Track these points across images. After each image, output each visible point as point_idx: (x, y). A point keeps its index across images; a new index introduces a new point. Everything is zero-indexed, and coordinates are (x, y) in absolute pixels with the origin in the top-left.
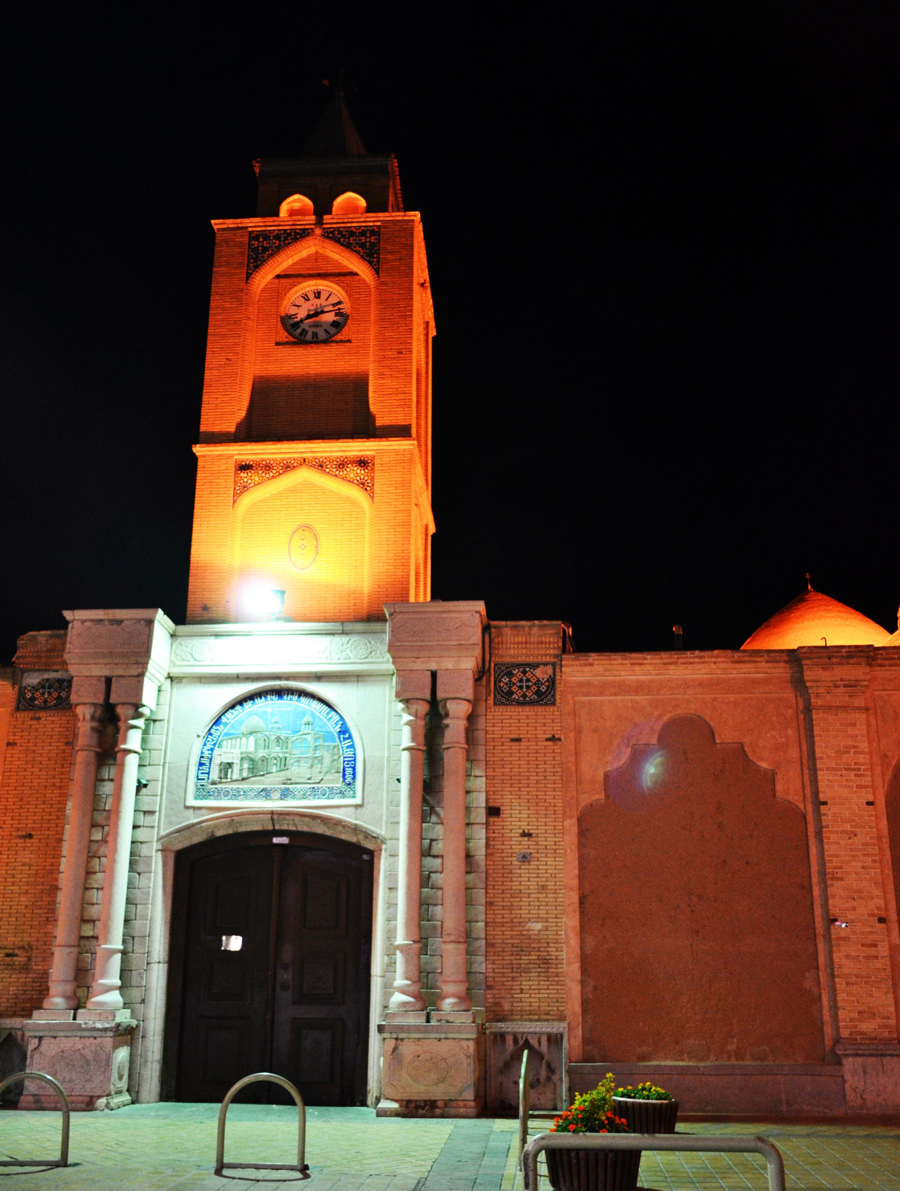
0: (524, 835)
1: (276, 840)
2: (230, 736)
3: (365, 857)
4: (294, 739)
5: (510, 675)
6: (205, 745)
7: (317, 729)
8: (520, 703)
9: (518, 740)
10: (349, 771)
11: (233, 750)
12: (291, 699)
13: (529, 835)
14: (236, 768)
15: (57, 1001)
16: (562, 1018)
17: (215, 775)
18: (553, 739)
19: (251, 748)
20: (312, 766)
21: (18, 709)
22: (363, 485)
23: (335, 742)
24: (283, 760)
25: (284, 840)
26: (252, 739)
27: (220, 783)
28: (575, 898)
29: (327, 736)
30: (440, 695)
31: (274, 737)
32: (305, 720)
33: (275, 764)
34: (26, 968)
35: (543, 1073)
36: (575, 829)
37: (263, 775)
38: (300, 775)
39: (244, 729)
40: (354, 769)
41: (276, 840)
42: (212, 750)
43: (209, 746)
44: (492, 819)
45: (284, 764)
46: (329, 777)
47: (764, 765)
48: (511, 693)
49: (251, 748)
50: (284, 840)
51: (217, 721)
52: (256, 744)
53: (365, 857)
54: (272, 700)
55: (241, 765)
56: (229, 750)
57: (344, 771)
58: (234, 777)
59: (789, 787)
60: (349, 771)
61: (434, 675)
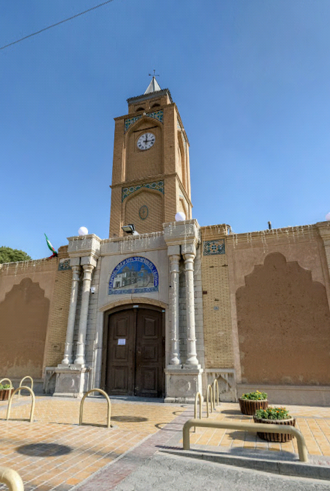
0: (216, 300)
1: (135, 306)
2: (118, 273)
3: (163, 311)
5: (209, 245)
8: (212, 254)
9: (213, 267)
13: (218, 300)
15: (67, 361)
16: (233, 367)
17: (114, 286)
18: (225, 266)
21: (59, 270)
22: (161, 190)
25: (137, 306)
30: (182, 253)
34: (60, 351)
35: (227, 389)
36: (234, 297)
41: (135, 306)
44: (205, 295)
47: (306, 269)
48: (209, 251)
50: (137, 306)
51: (115, 269)
53: (163, 311)
59: (317, 276)
60: (156, 281)
61: (180, 246)
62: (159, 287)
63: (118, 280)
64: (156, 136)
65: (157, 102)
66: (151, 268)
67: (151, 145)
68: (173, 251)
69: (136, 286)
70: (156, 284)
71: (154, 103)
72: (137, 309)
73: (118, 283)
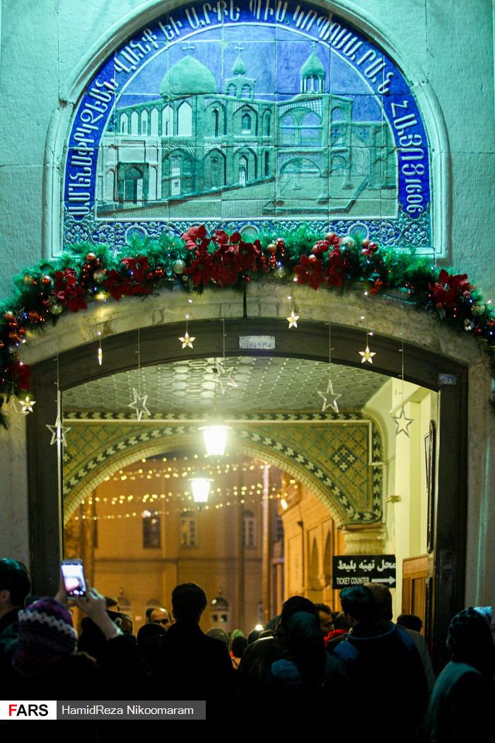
4: (283, 110)
6: (78, 123)
7: (335, 88)
10: (414, 184)
11: (144, 137)
12: (271, 19)
20: (328, 173)
23: (379, 119)
24: (262, 159)
26: (186, 111)
27: (120, 210)
29: (358, 104)
31: (236, 106)
32: (305, 67)
33: (242, 168)
37: (218, 193)
38: (302, 192)
39: (164, 86)
40: (425, 180)
42: (96, 135)
43: (88, 127)
45: (264, 167)
46: (367, 196)
49: (186, 132)
52: (195, 120)
54: (227, 19)
55: (166, 171)
56: (134, 135)
57: (402, 184)
58: (151, 197)
60: (414, 184)
63: (129, 156)
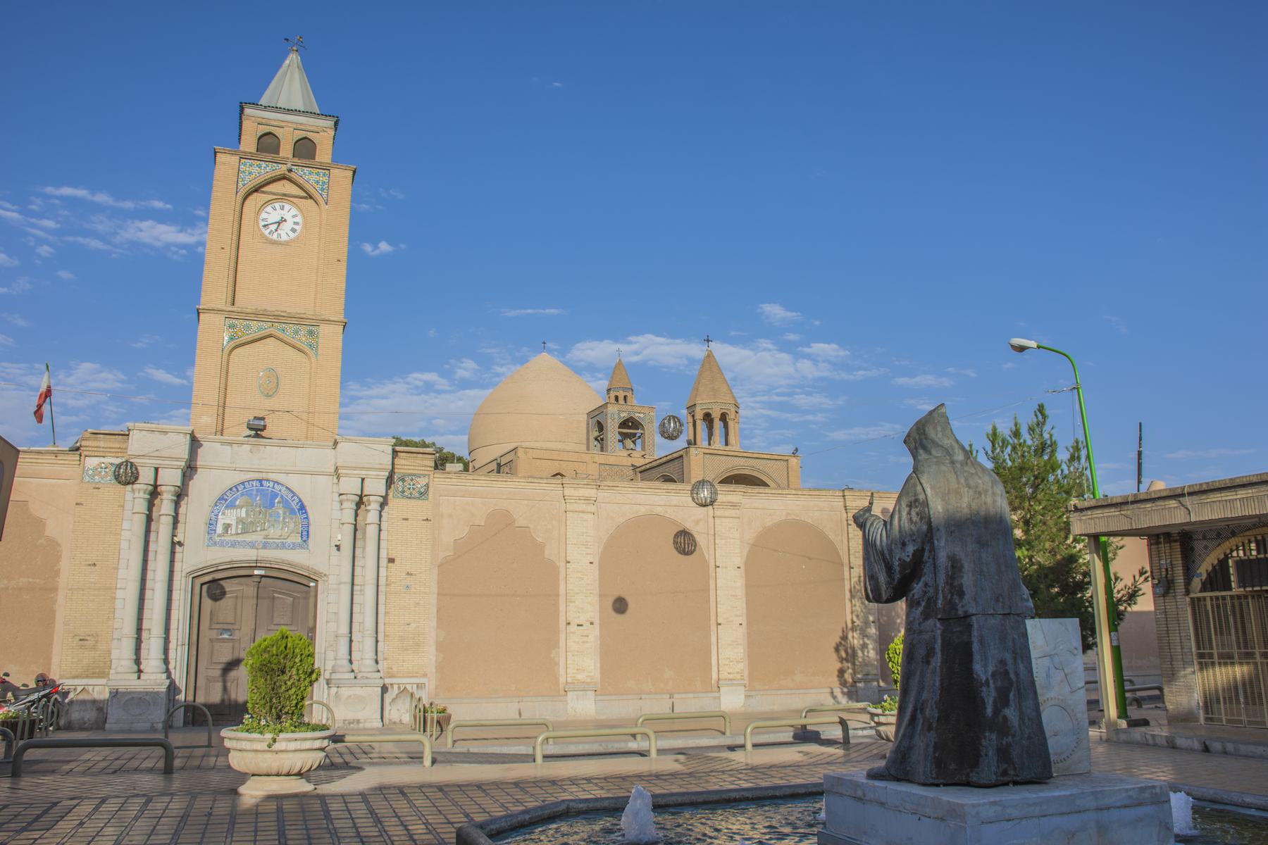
1: (256, 572)
3: (312, 584)
14: (234, 528)
16: (425, 675)
17: (220, 529)
19: (244, 515)
28: (435, 610)
30: (365, 492)
41: (256, 572)
50: (262, 572)
51: (221, 498)
62: (310, 541)
63: (228, 522)
64: (304, 217)
65: (310, 135)
66: (294, 505)
67: (292, 235)
68: (350, 485)
69: (266, 537)
70: (305, 535)
71: (304, 134)
72: (262, 576)
73: (227, 527)
